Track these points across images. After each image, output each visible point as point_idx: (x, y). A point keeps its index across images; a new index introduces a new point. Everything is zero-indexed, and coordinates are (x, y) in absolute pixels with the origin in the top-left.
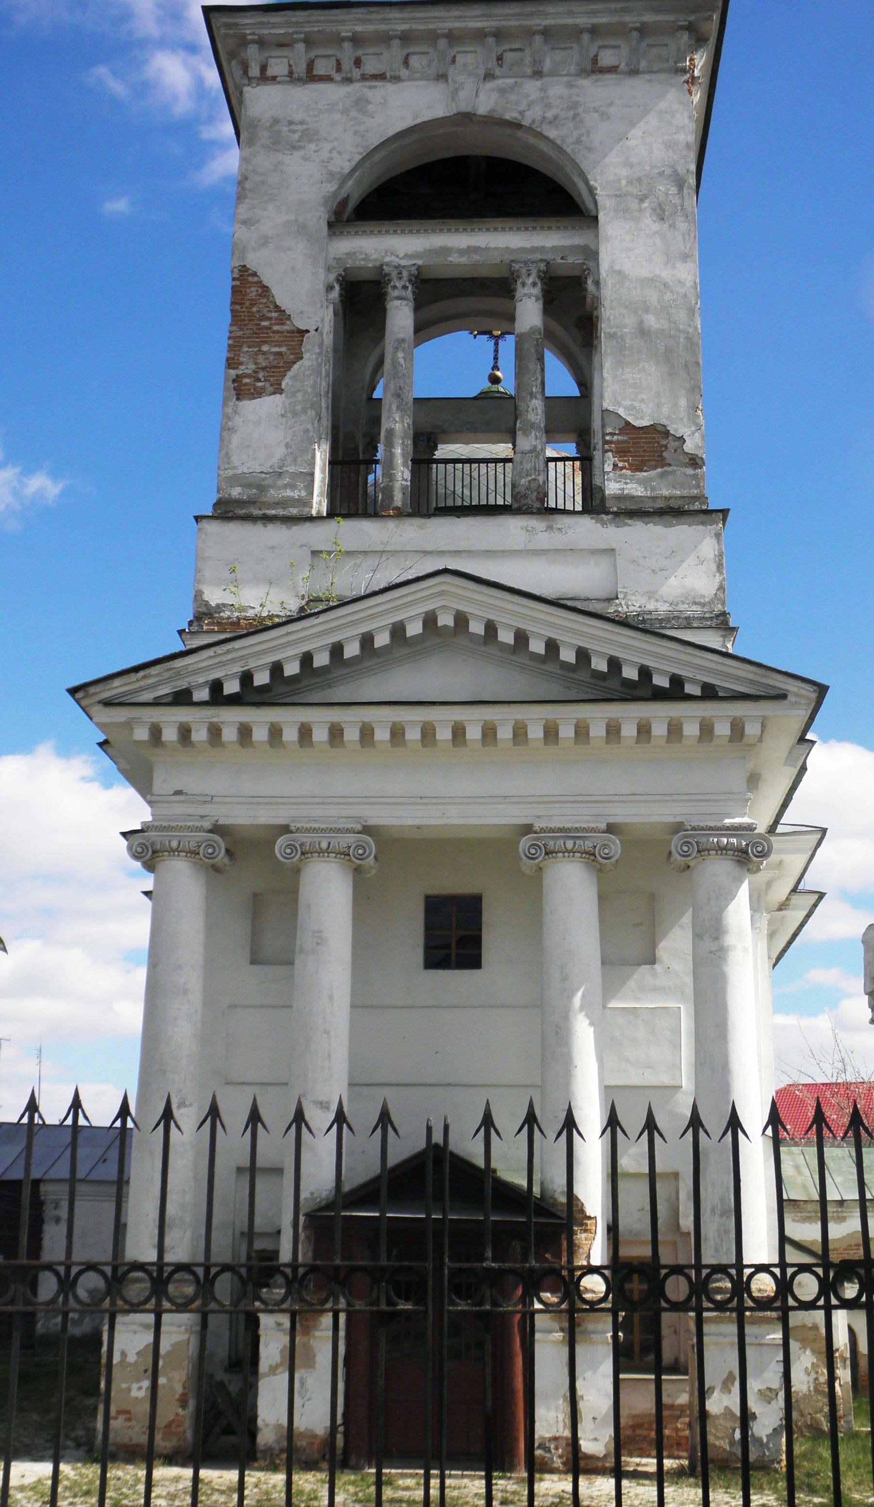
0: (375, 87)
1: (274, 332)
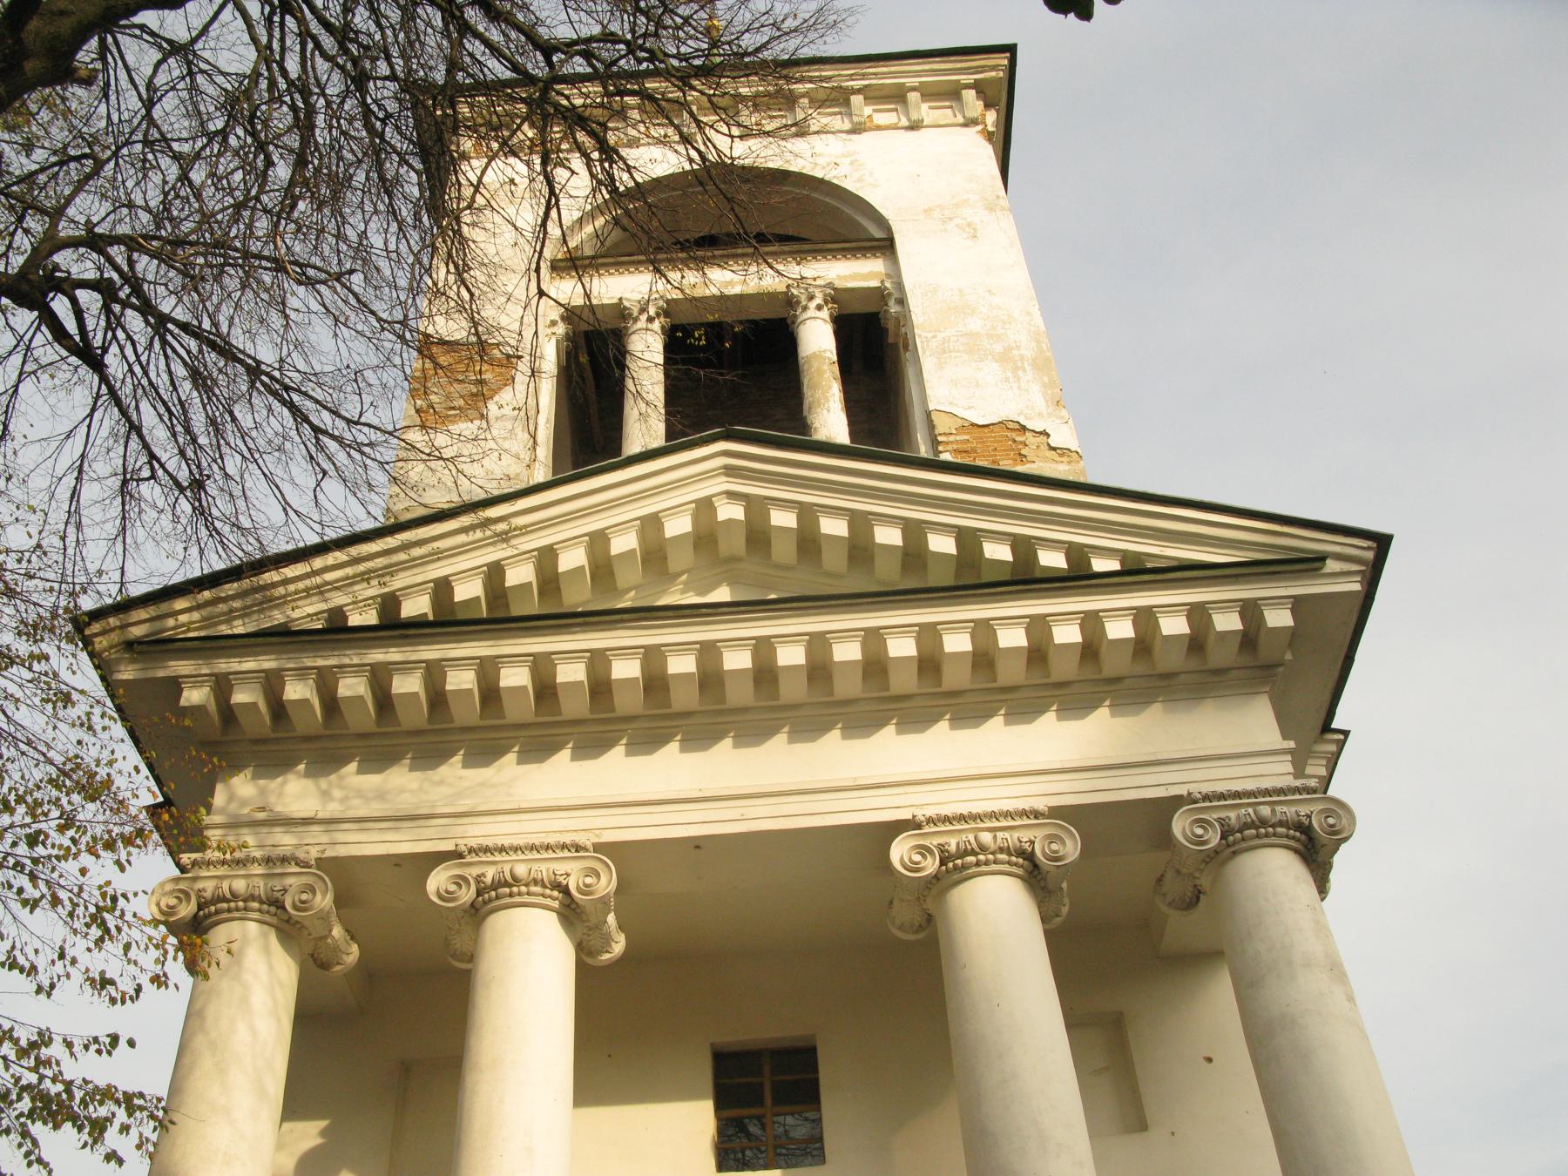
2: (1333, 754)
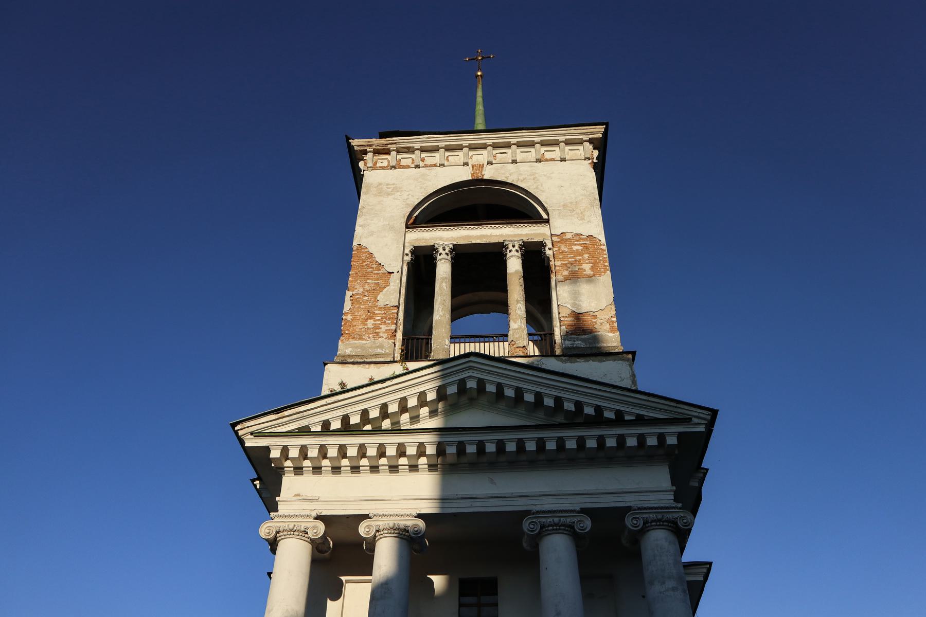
0: (431, 169)
1: (375, 274)
2: (701, 477)
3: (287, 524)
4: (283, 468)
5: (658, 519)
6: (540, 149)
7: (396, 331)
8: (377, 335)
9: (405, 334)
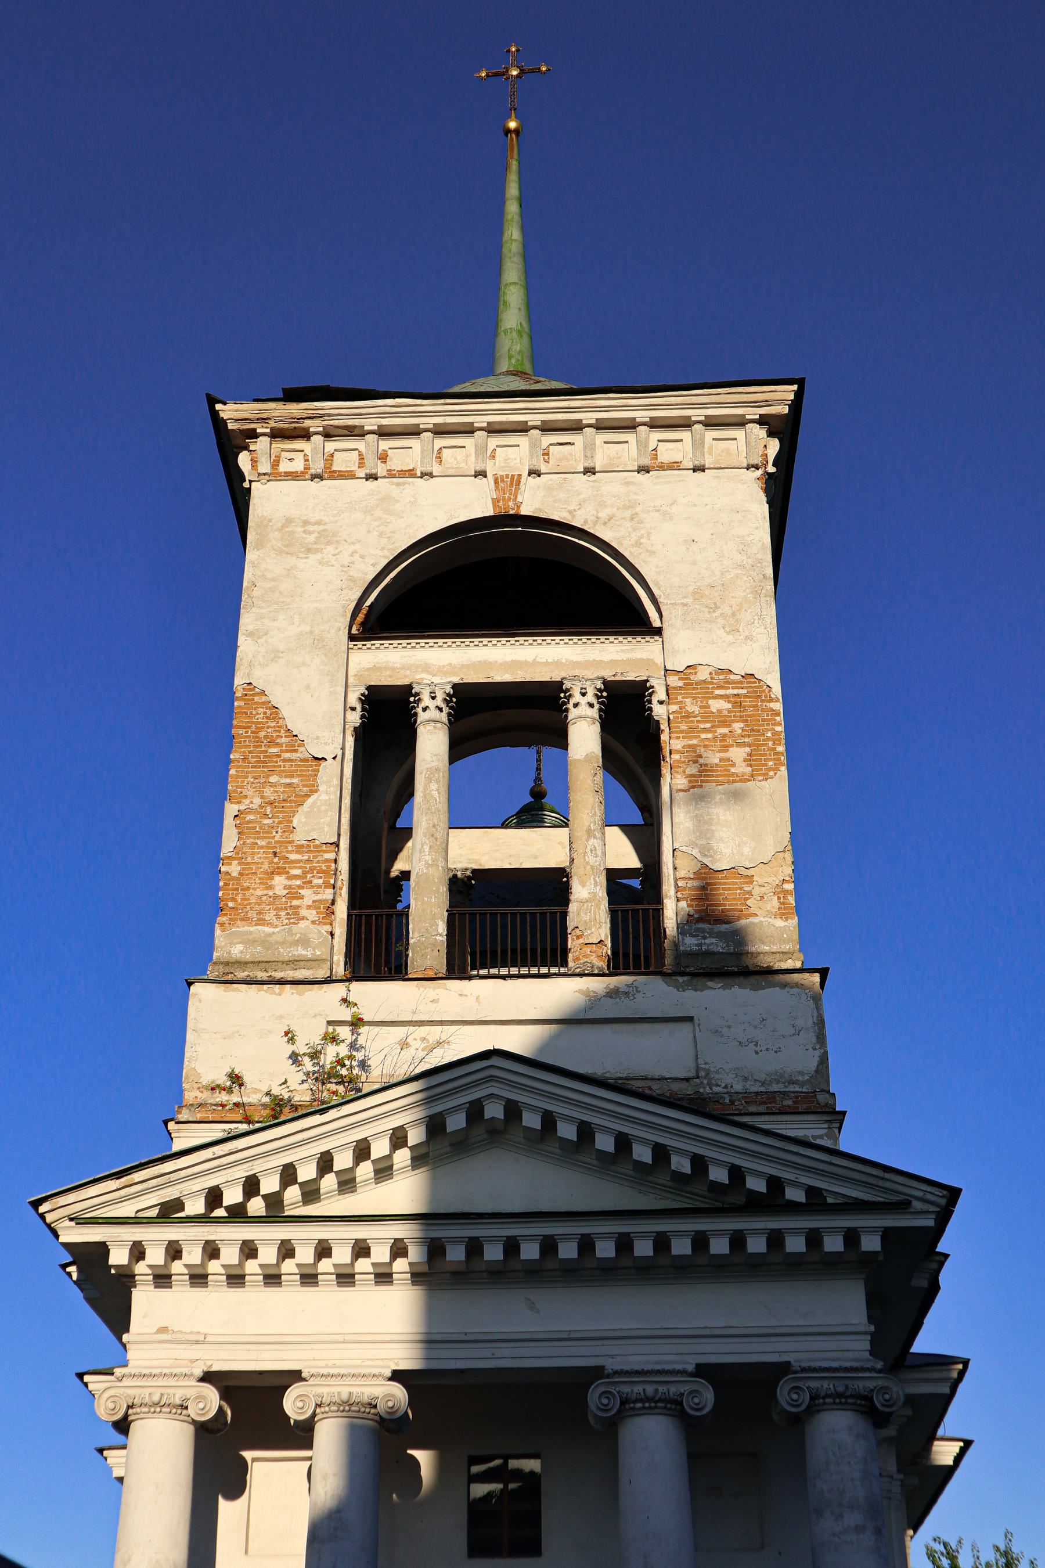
0: (404, 484)
1: (284, 760)
2: (934, 1270)
3: (147, 1391)
4: (134, 1276)
5: (837, 1393)
6: (647, 440)
7: (333, 903)
8: (295, 914)
9: (353, 903)
